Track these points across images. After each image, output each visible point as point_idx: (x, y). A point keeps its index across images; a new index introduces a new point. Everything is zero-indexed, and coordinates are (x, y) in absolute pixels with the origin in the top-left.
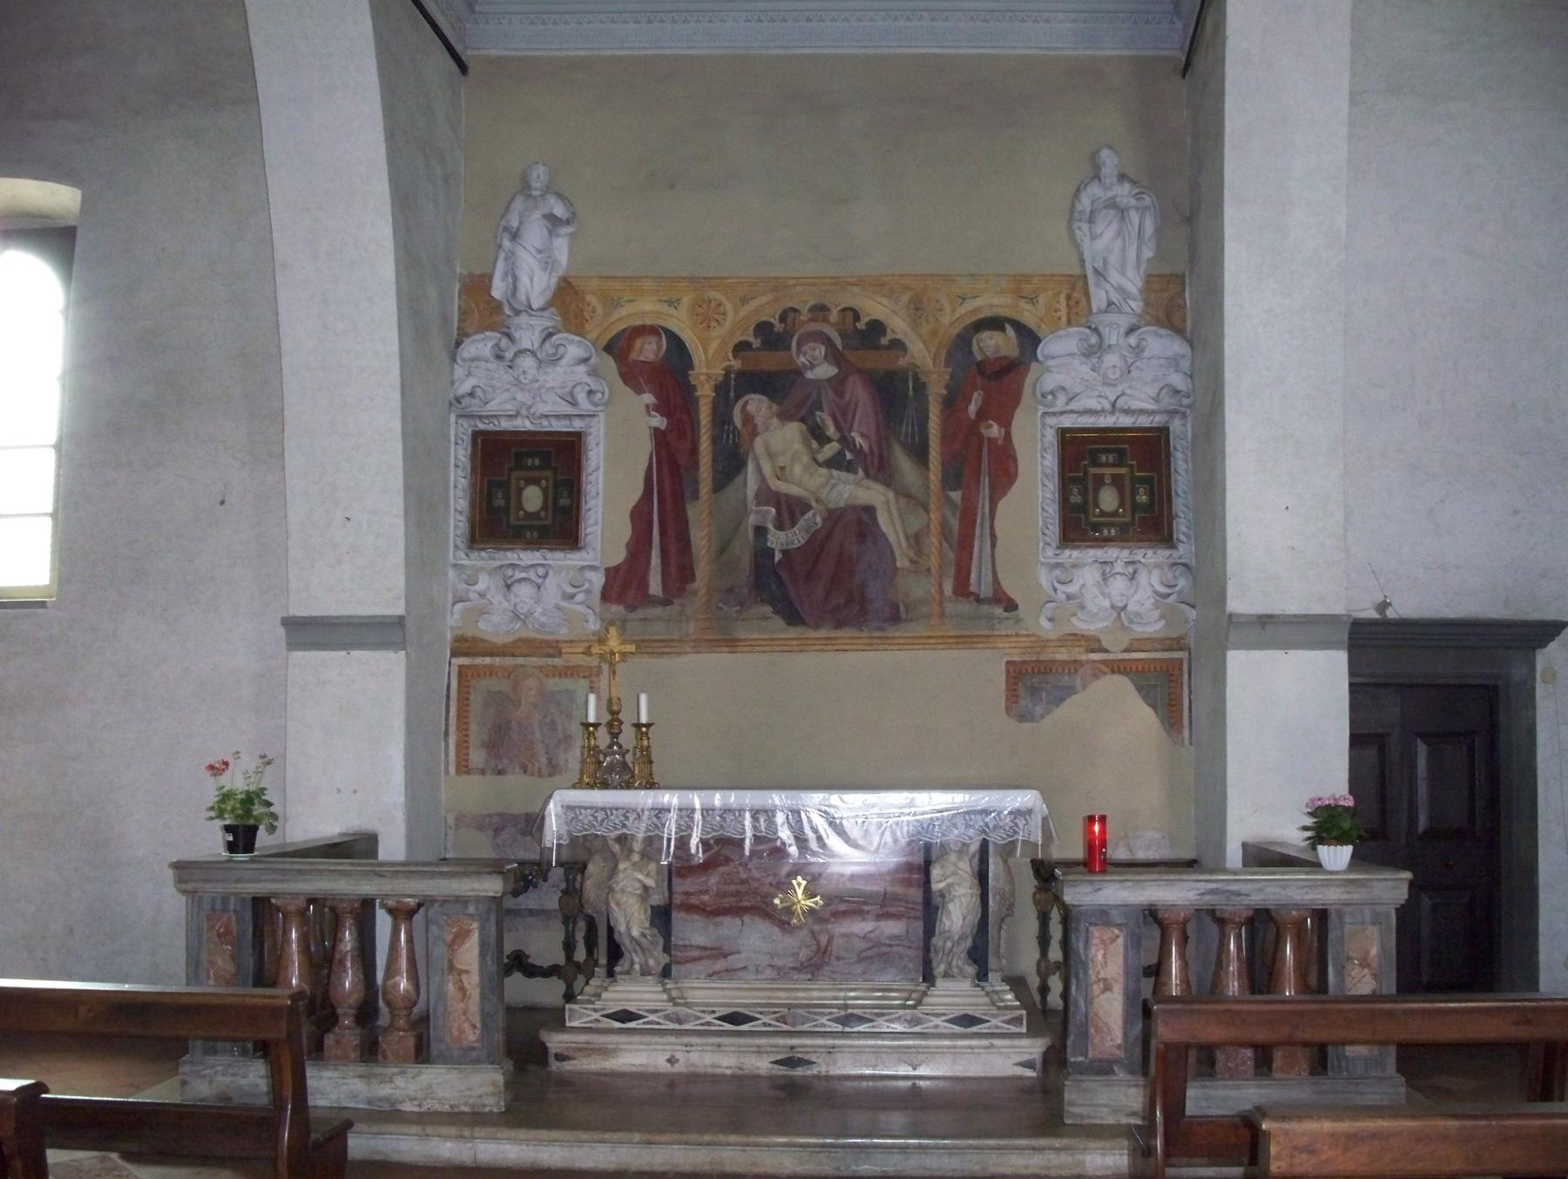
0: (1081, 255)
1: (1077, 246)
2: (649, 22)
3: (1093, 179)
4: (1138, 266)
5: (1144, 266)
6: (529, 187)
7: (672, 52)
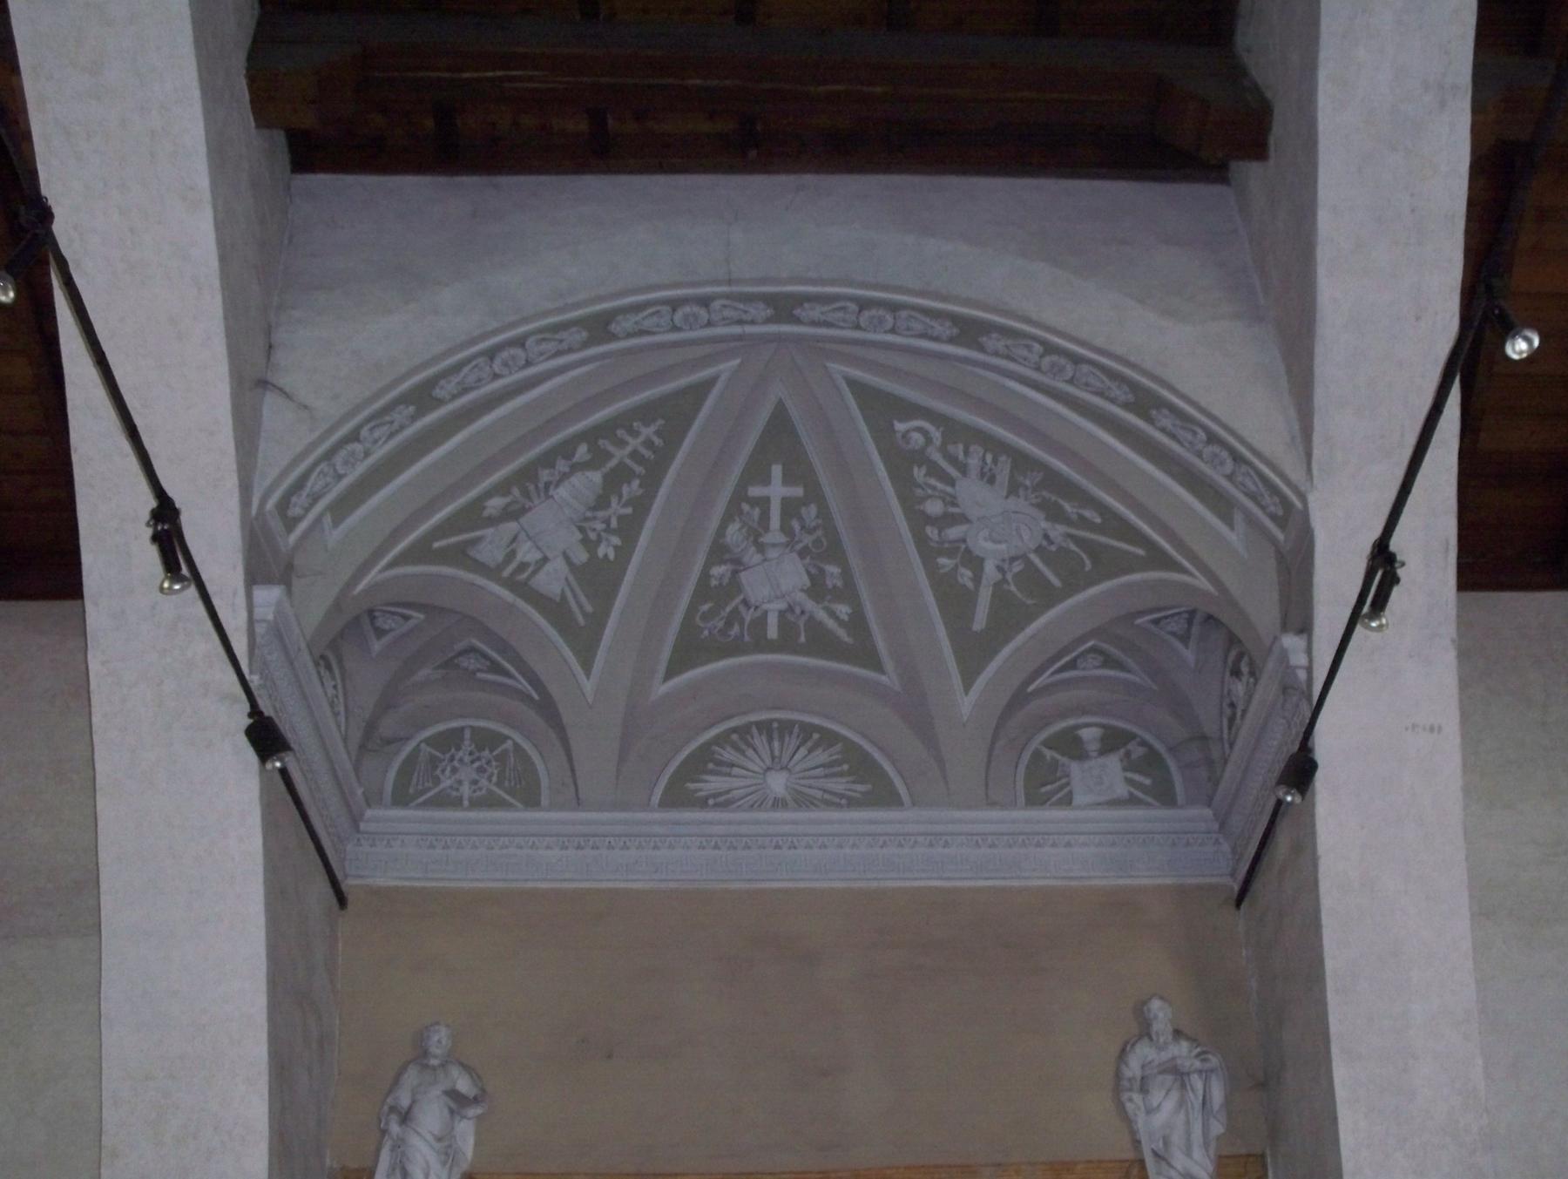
0: (1133, 1133)
1: (1127, 1120)
2: (579, 847)
3: (1140, 1037)
4: (1206, 1145)
5: (1213, 1145)
6: (425, 1054)
7: (610, 885)
